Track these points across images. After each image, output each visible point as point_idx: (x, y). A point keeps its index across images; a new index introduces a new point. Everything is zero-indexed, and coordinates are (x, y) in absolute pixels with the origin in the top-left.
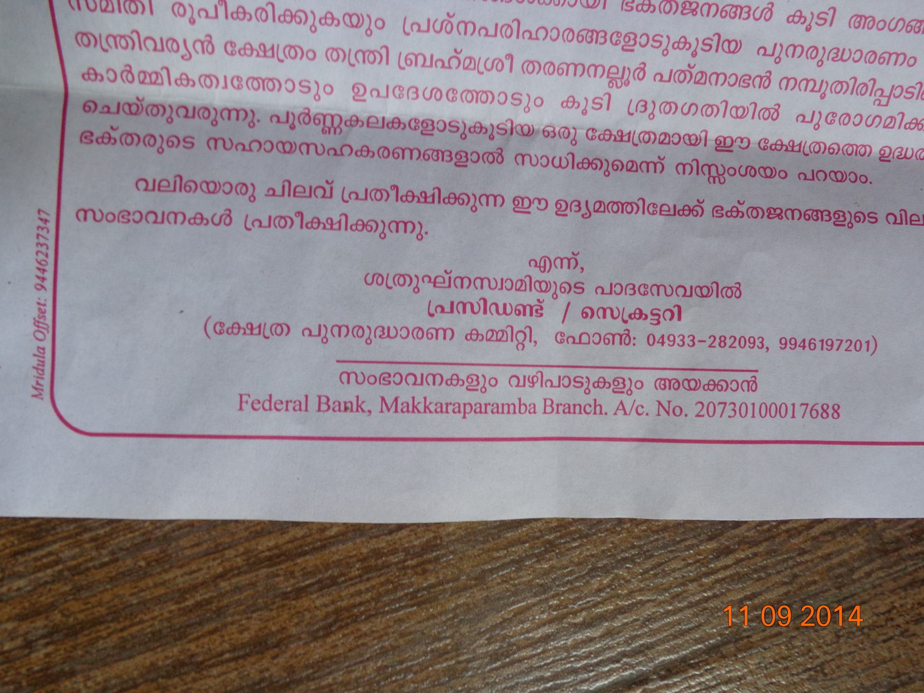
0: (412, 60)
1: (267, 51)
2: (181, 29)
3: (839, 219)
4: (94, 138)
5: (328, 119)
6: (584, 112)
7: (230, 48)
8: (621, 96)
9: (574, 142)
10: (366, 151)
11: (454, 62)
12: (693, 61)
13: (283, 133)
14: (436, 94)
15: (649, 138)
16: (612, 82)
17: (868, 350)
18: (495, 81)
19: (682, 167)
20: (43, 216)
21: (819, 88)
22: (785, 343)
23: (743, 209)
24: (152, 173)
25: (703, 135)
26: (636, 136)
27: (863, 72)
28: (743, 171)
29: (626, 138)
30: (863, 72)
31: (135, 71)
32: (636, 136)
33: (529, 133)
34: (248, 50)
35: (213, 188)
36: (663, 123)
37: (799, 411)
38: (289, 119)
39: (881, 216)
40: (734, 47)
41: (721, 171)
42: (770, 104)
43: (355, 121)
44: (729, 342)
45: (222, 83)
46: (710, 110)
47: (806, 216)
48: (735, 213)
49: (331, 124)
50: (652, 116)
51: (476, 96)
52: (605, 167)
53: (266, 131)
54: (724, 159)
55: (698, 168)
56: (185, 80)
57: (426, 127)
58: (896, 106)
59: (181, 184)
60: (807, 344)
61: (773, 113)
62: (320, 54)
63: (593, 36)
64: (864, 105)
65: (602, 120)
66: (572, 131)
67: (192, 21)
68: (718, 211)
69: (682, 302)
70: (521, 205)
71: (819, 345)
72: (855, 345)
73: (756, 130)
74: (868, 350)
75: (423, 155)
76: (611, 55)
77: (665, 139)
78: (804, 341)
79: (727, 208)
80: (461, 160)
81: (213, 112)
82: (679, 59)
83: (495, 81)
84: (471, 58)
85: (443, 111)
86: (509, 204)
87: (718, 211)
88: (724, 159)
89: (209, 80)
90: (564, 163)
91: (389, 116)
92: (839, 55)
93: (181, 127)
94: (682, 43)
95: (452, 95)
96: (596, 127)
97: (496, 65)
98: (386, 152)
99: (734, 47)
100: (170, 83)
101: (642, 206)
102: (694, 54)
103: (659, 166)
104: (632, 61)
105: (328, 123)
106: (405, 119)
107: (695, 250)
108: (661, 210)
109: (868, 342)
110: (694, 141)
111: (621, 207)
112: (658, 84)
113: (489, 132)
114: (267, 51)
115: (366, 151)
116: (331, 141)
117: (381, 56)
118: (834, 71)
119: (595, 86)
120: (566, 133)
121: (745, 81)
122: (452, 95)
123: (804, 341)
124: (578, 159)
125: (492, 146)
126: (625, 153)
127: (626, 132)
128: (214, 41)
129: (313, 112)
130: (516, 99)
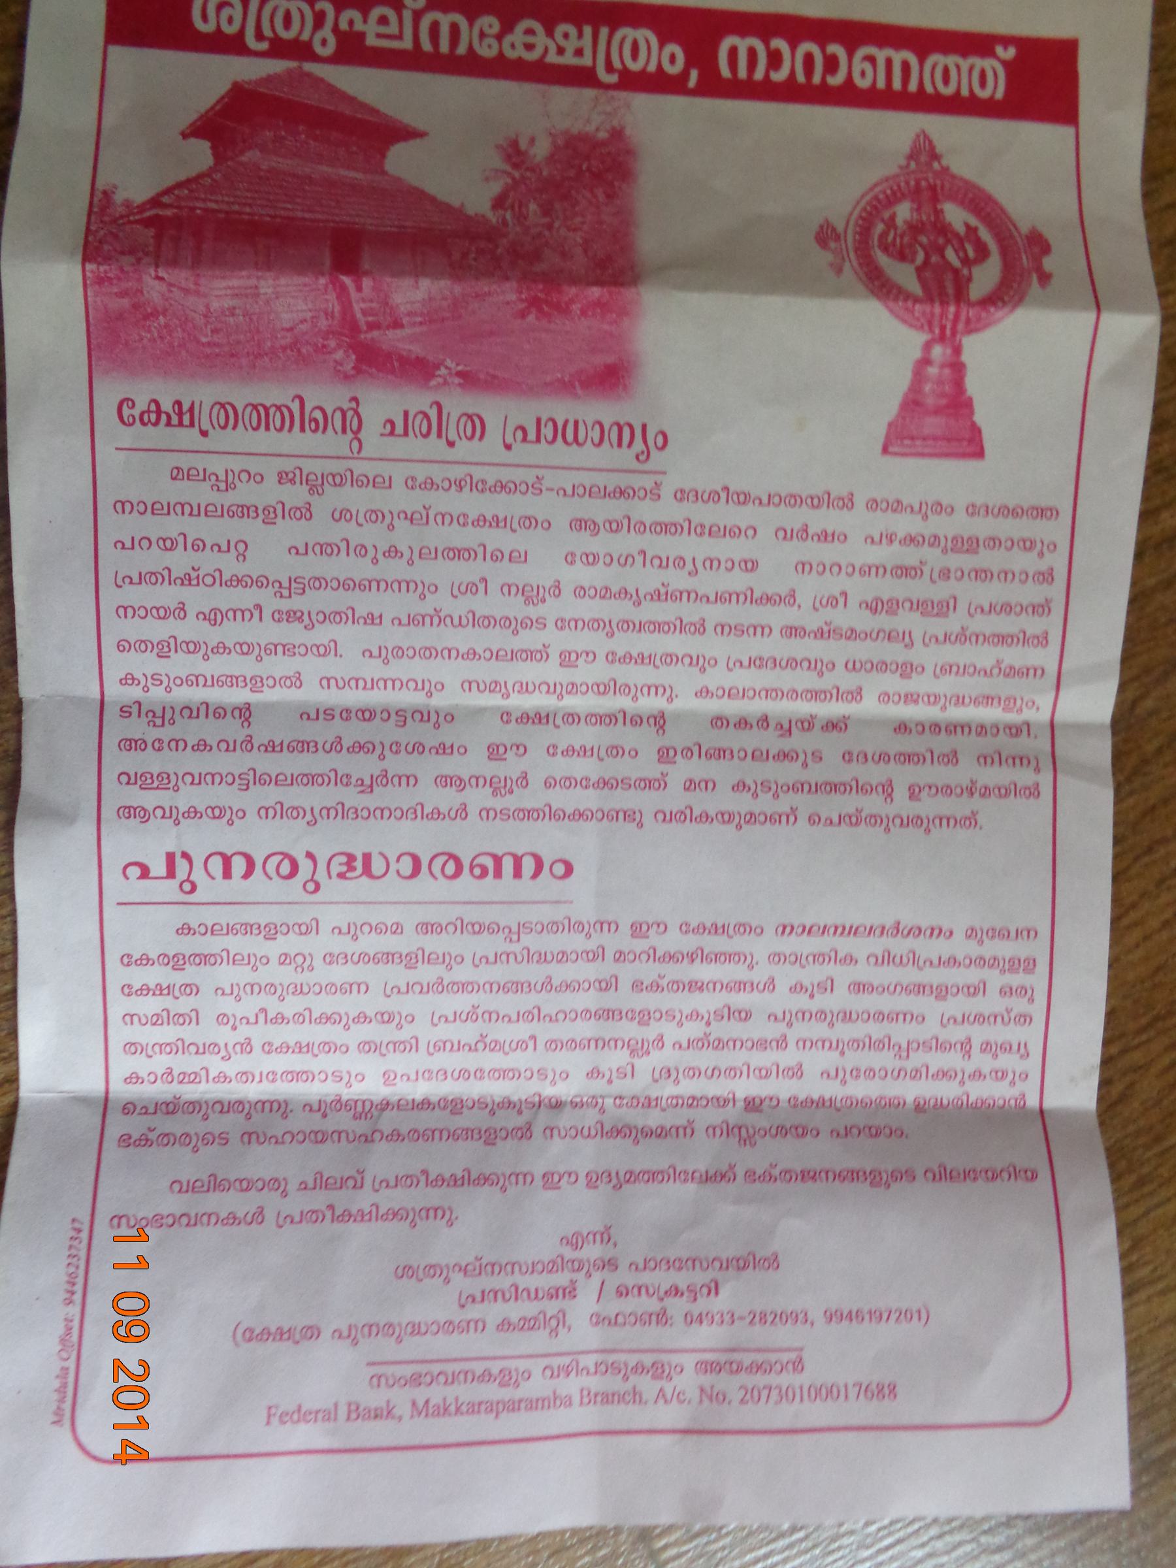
0: (440, 1046)
1: (302, 1048)
2: (224, 1035)
3: (875, 1178)
4: (132, 1141)
5: (359, 1104)
6: (610, 1081)
7: (268, 1048)
8: (644, 1065)
9: (602, 1111)
10: (396, 1136)
11: (480, 1046)
12: (708, 1030)
13: (315, 1122)
14: (464, 1074)
15: (677, 1102)
16: (633, 1052)
17: (920, 1319)
18: (519, 1060)
19: (712, 1130)
20: (77, 1225)
21: (838, 1046)
22: (832, 1316)
23: (776, 1172)
24: (187, 1174)
25: (731, 1096)
26: (664, 1101)
27: (876, 1030)
28: (774, 1131)
29: (653, 1103)
30: (876, 1030)
31: (175, 1073)
32: (664, 1101)
33: (557, 1105)
34: (285, 1048)
35: (246, 1184)
36: (688, 1087)
37: (852, 1393)
38: (321, 1108)
39: (919, 1173)
40: (745, 1015)
41: (751, 1131)
42: (792, 1063)
43: (386, 1105)
44: (770, 1319)
45: (257, 1079)
46: (733, 1072)
47: (840, 1176)
48: (768, 1177)
49: (365, 1110)
50: (677, 1081)
51: (503, 1074)
52: (634, 1134)
53: (299, 1122)
54: (753, 1119)
55: (729, 1130)
56: (223, 1078)
57: (455, 1106)
58: (917, 1059)
59: (216, 1184)
60: (853, 1316)
61: (797, 1072)
62: (353, 1047)
63: (608, 1014)
64: (884, 1059)
65: (627, 1087)
66: (600, 1101)
67: (234, 1028)
68: (750, 1176)
69: (719, 1276)
70: (550, 1180)
71: (867, 1317)
72: (905, 1315)
73: (784, 1088)
74: (920, 1319)
75: (453, 1136)
76: (629, 1030)
77: (694, 1101)
78: (850, 1312)
79: (759, 1172)
80: (490, 1137)
81: (247, 1106)
82: (694, 1029)
83: (519, 1060)
84: (496, 1042)
85: (474, 1089)
86: (538, 1181)
87: (750, 1176)
88: (753, 1119)
89: (246, 1076)
90: (593, 1132)
91: (419, 1097)
92: (847, 1017)
93: (218, 1123)
94: (695, 1015)
95: (479, 1074)
96: (624, 1094)
97: (521, 1045)
98: (417, 1135)
99: (745, 1015)
100: (207, 1081)
101: (674, 1175)
102: (708, 1024)
103: (689, 1131)
104: (651, 1032)
105: (359, 1109)
106: (434, 1099)
107: (728, 1219)
108: (689, 1176)
109: (919, 1312)
110: (722, 1102)
111: (653, 1176)
112: (677, 1052)
113: (518, 1107)
114: (302, 1048)
115: (396, 1136)
116: (362, 1127)
117: (412, 1045)
118: (845, 1032)
119: (617, 1058)
120: (595, 1102)
121: (761, 1044)
122: (479, 1074)
123: (850, 1312)
124: (607, 1128)
125: (520, 1121)
126: (654, 1119)
127: (653, 1096)
128: (253, 1043)
129: (345, 1098)
130: (542, 1073)
